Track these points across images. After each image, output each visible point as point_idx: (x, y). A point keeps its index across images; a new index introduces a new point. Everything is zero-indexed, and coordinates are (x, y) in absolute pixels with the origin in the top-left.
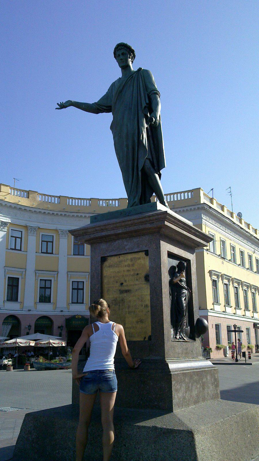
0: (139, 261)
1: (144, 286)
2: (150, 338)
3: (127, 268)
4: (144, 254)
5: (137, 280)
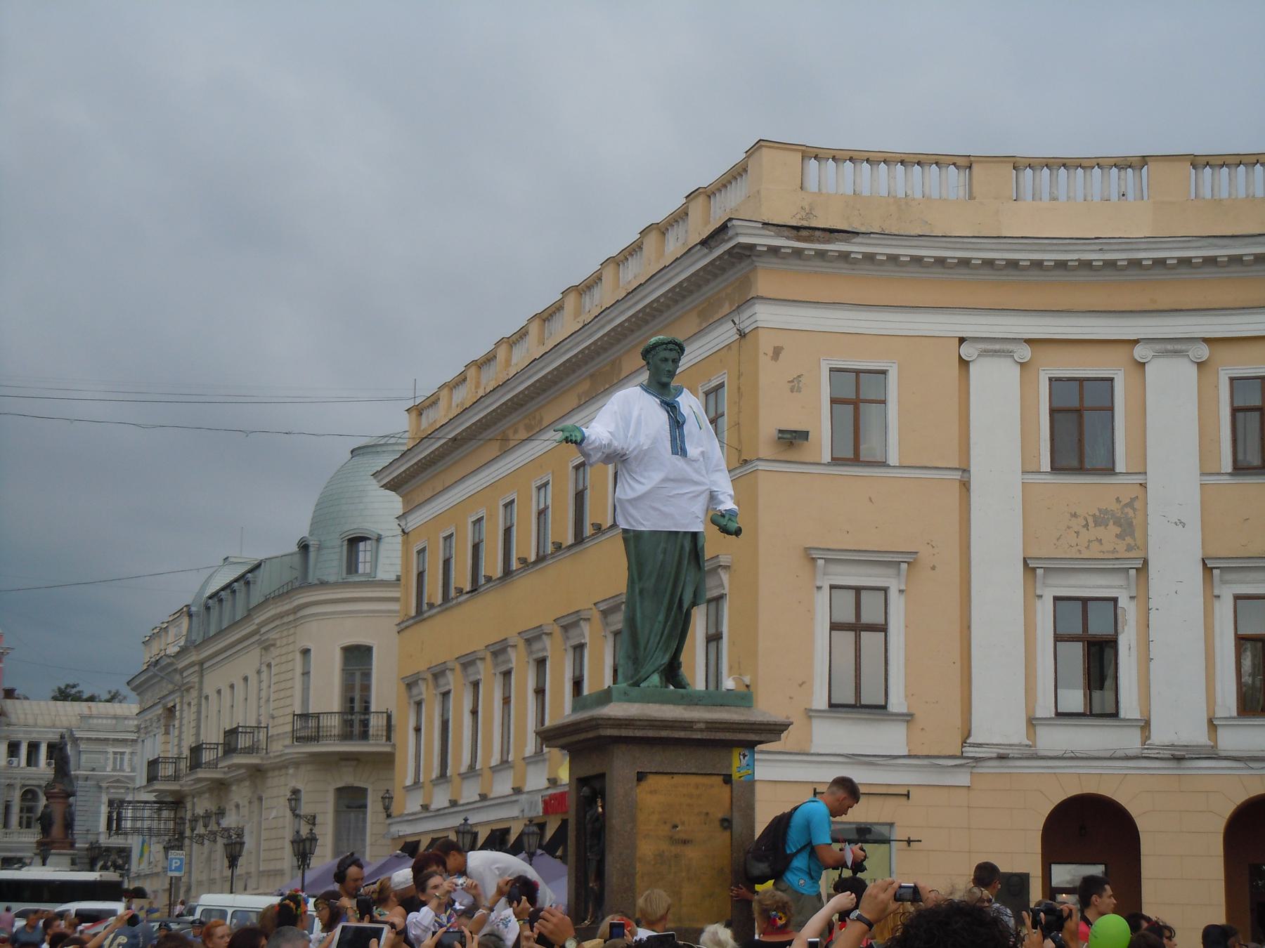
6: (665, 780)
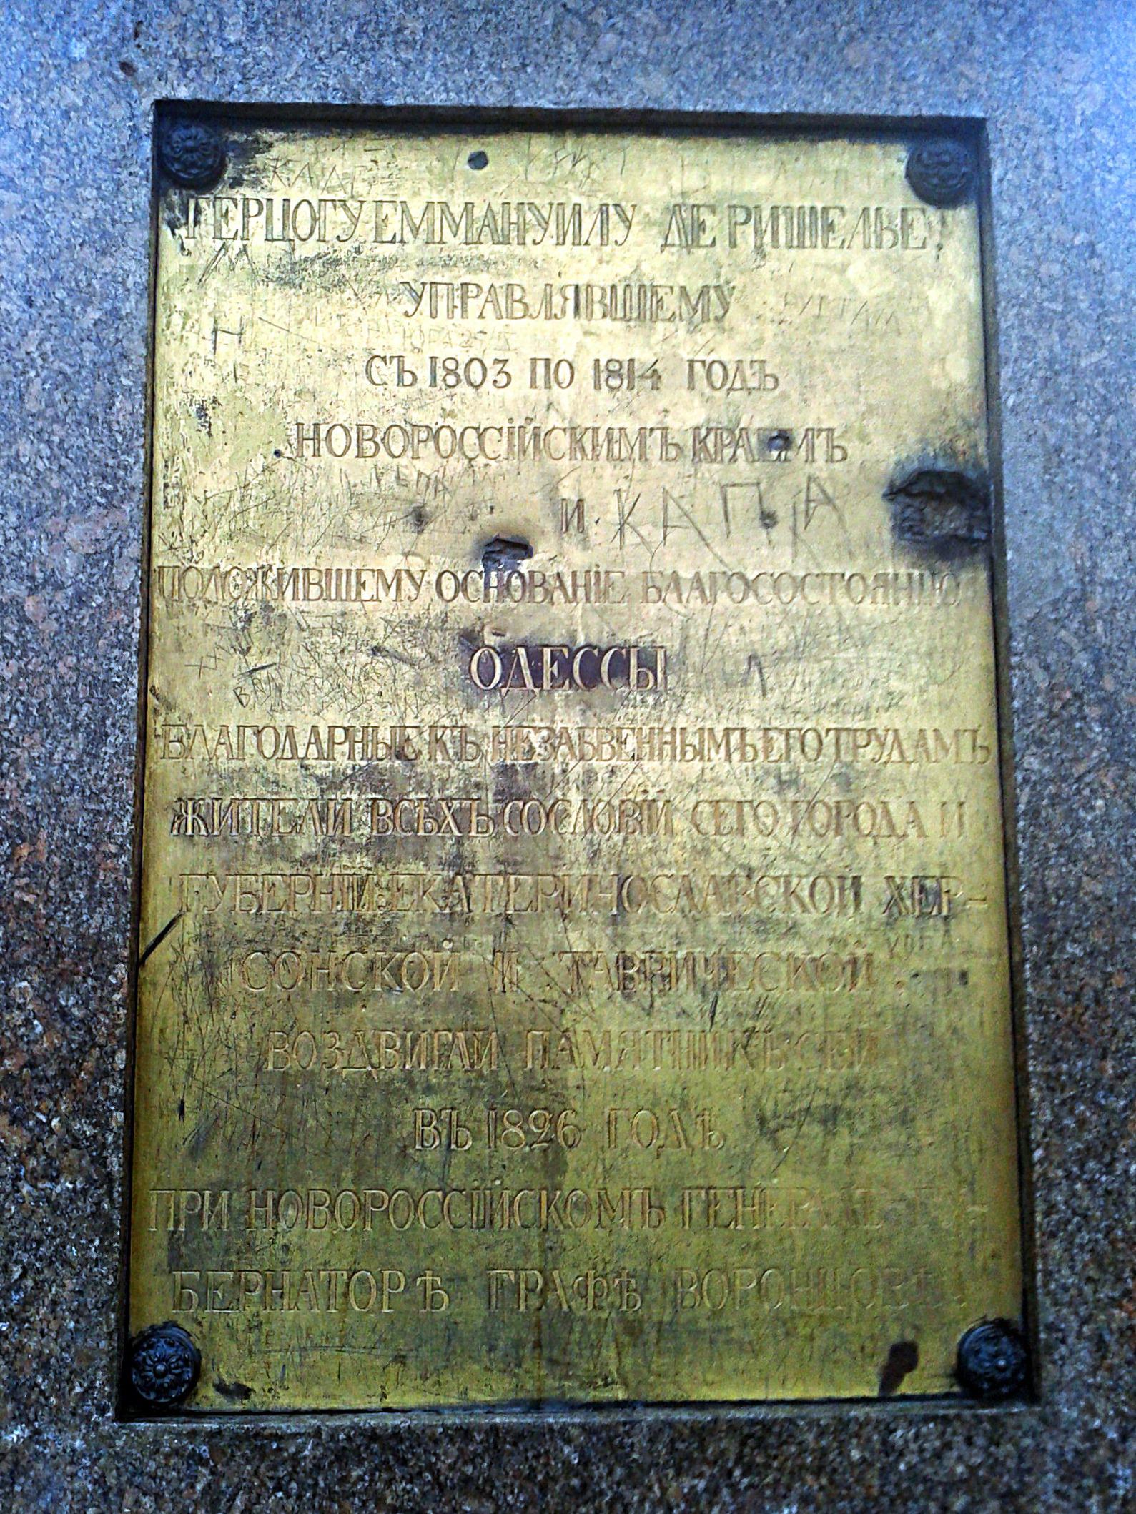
0: (809, 265)
1: (874, 609)
2: (1003, 1369)
3: (615, 340)
4: (901, 169)
5: (768, 520)
6: (410, 176)
